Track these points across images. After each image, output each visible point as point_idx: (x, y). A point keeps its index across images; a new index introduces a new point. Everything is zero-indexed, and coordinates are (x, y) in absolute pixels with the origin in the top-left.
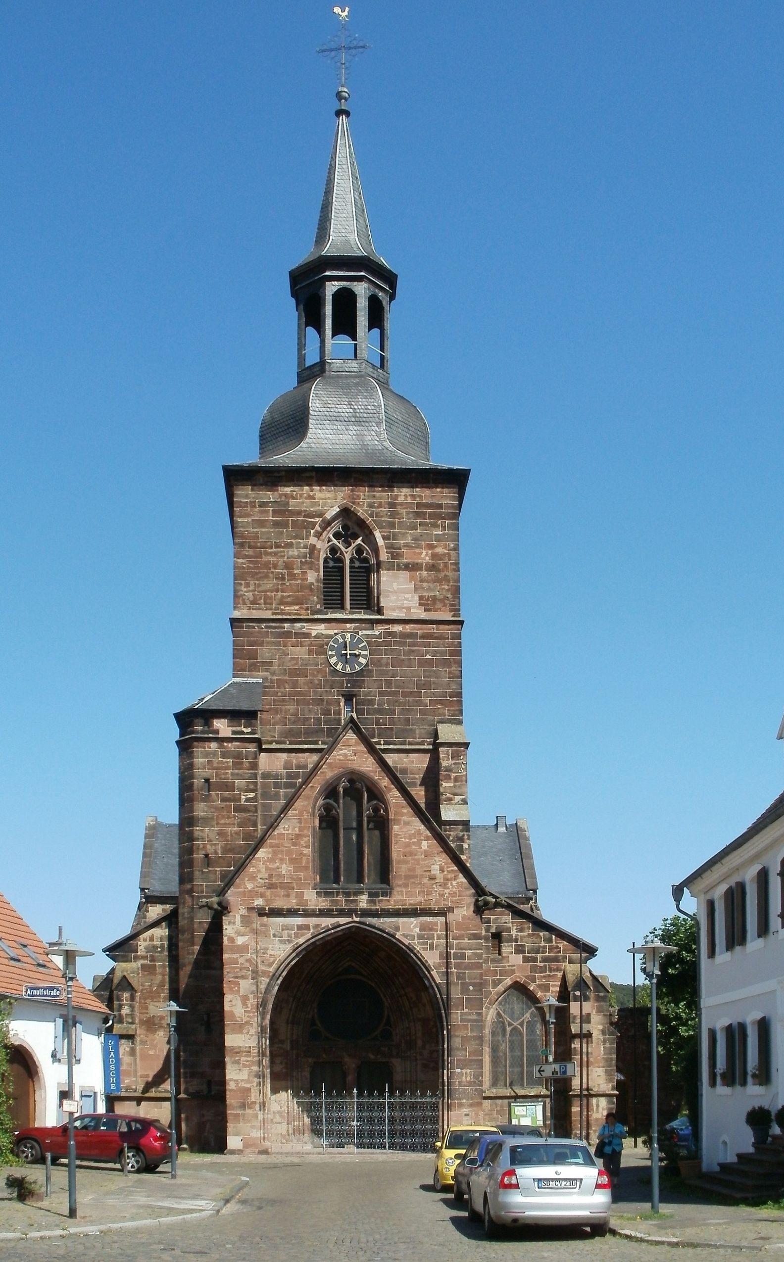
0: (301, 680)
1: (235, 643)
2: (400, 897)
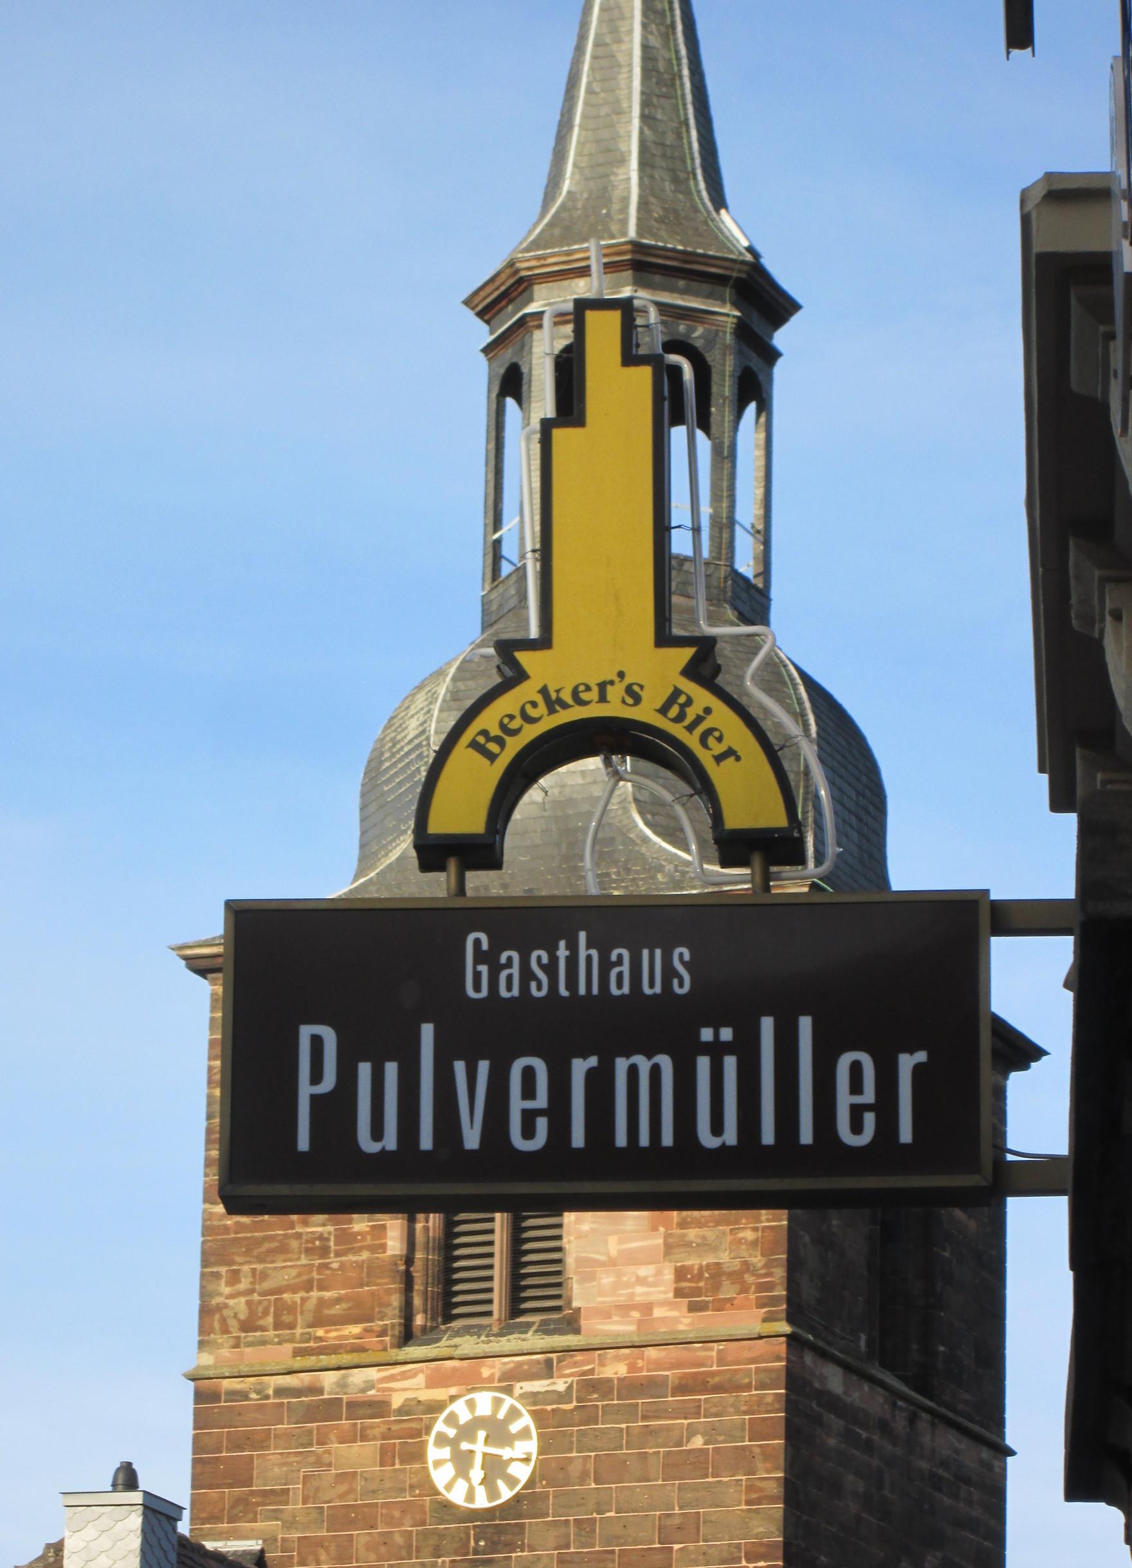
0: (361, 1536)
1: (198, 1445)
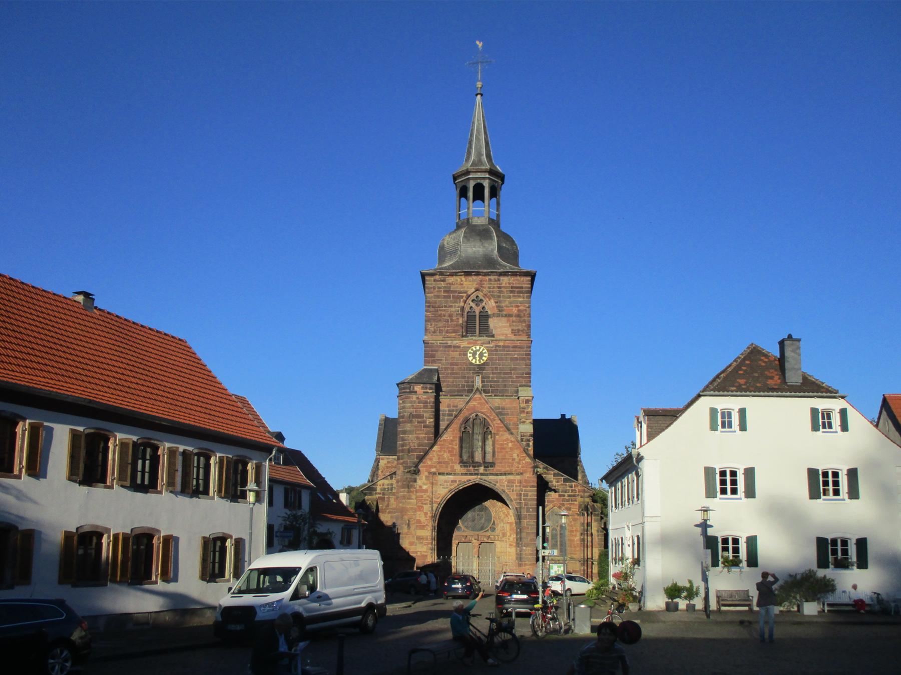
2: (498, 468)
